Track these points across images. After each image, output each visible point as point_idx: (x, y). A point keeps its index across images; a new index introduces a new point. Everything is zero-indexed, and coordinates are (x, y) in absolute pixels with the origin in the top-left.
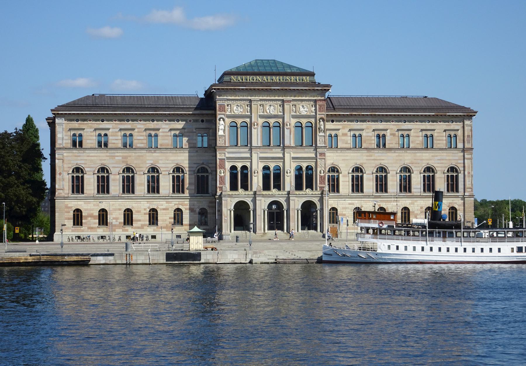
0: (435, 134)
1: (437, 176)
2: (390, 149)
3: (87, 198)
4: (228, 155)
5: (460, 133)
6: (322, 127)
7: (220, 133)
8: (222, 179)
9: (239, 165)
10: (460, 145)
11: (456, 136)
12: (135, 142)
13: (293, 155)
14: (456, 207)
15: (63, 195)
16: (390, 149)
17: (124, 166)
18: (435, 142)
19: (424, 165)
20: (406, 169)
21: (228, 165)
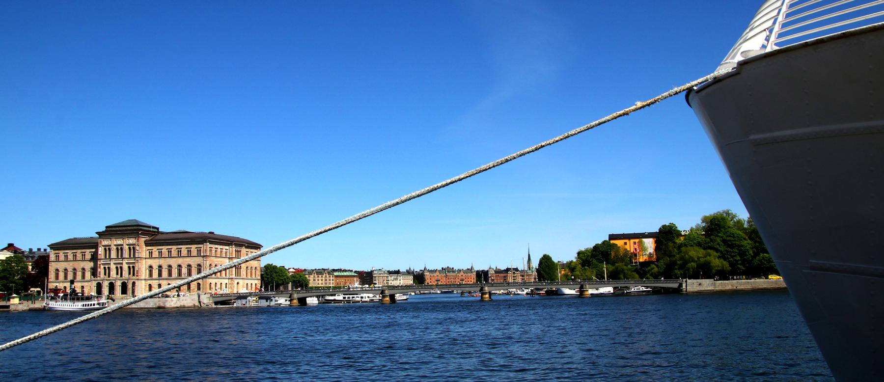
0: (192, 250)
1: (192, 269)
2: (173, 257)
3: (164, 279)
4: (102, 262)
5: (202, 249)
6: (138, 249)
7: (100, 253)
8: (100, 272)
9: (107, 266)
10: (202, 254)
11: (200, 250)
12: (77, 257)
13: (127, 261)
14: (200, 282)
15: (51, 281)
16: (173, 257)
17: (72, 268)
18: (192, 253)
19: (187, 263)
20: (180, 266)
21: (102, 267)
